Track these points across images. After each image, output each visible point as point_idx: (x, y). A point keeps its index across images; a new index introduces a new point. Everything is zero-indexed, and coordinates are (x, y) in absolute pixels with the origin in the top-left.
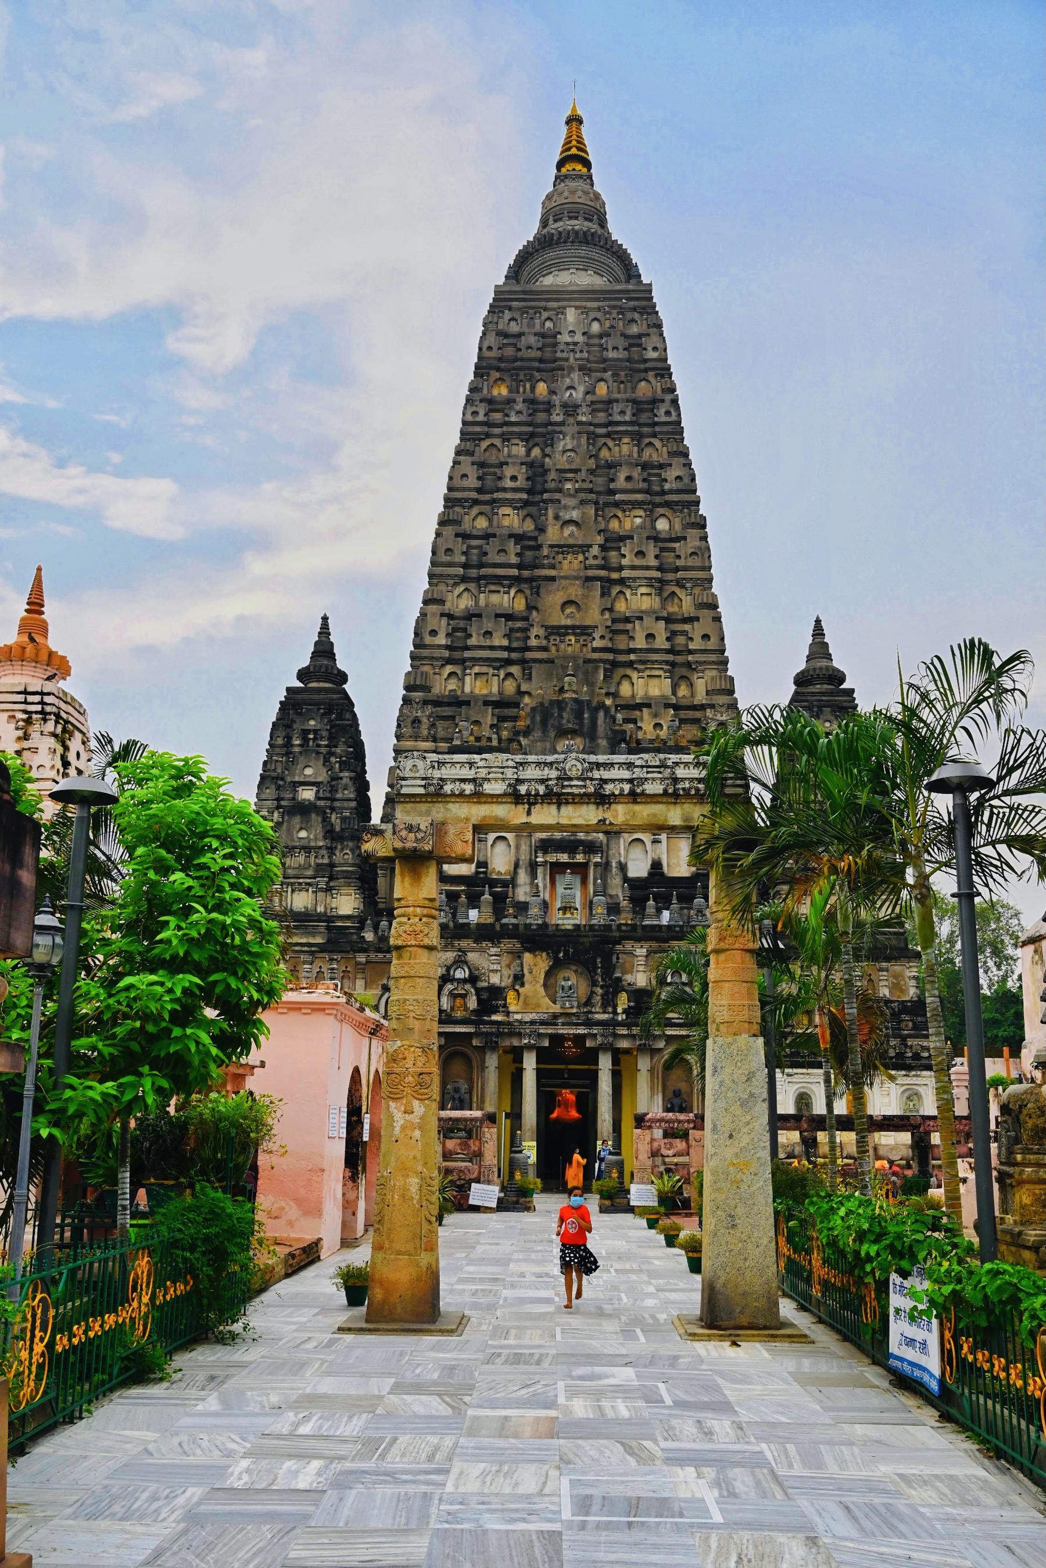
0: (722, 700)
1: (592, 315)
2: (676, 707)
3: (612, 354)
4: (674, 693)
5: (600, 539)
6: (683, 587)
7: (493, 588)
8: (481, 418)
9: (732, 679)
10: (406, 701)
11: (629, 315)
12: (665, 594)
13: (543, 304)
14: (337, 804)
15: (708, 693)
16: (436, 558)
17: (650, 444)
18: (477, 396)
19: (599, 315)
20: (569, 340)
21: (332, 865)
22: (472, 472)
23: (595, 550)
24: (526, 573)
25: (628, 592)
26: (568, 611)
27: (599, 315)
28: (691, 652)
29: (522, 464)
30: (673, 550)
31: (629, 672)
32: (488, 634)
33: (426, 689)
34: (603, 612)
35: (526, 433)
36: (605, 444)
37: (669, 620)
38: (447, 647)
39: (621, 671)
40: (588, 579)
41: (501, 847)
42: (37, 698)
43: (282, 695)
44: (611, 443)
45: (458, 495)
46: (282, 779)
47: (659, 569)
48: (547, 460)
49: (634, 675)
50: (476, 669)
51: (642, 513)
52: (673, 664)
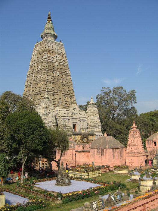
23: (61, 80)
40: (61, 84)
50: (50, 94)
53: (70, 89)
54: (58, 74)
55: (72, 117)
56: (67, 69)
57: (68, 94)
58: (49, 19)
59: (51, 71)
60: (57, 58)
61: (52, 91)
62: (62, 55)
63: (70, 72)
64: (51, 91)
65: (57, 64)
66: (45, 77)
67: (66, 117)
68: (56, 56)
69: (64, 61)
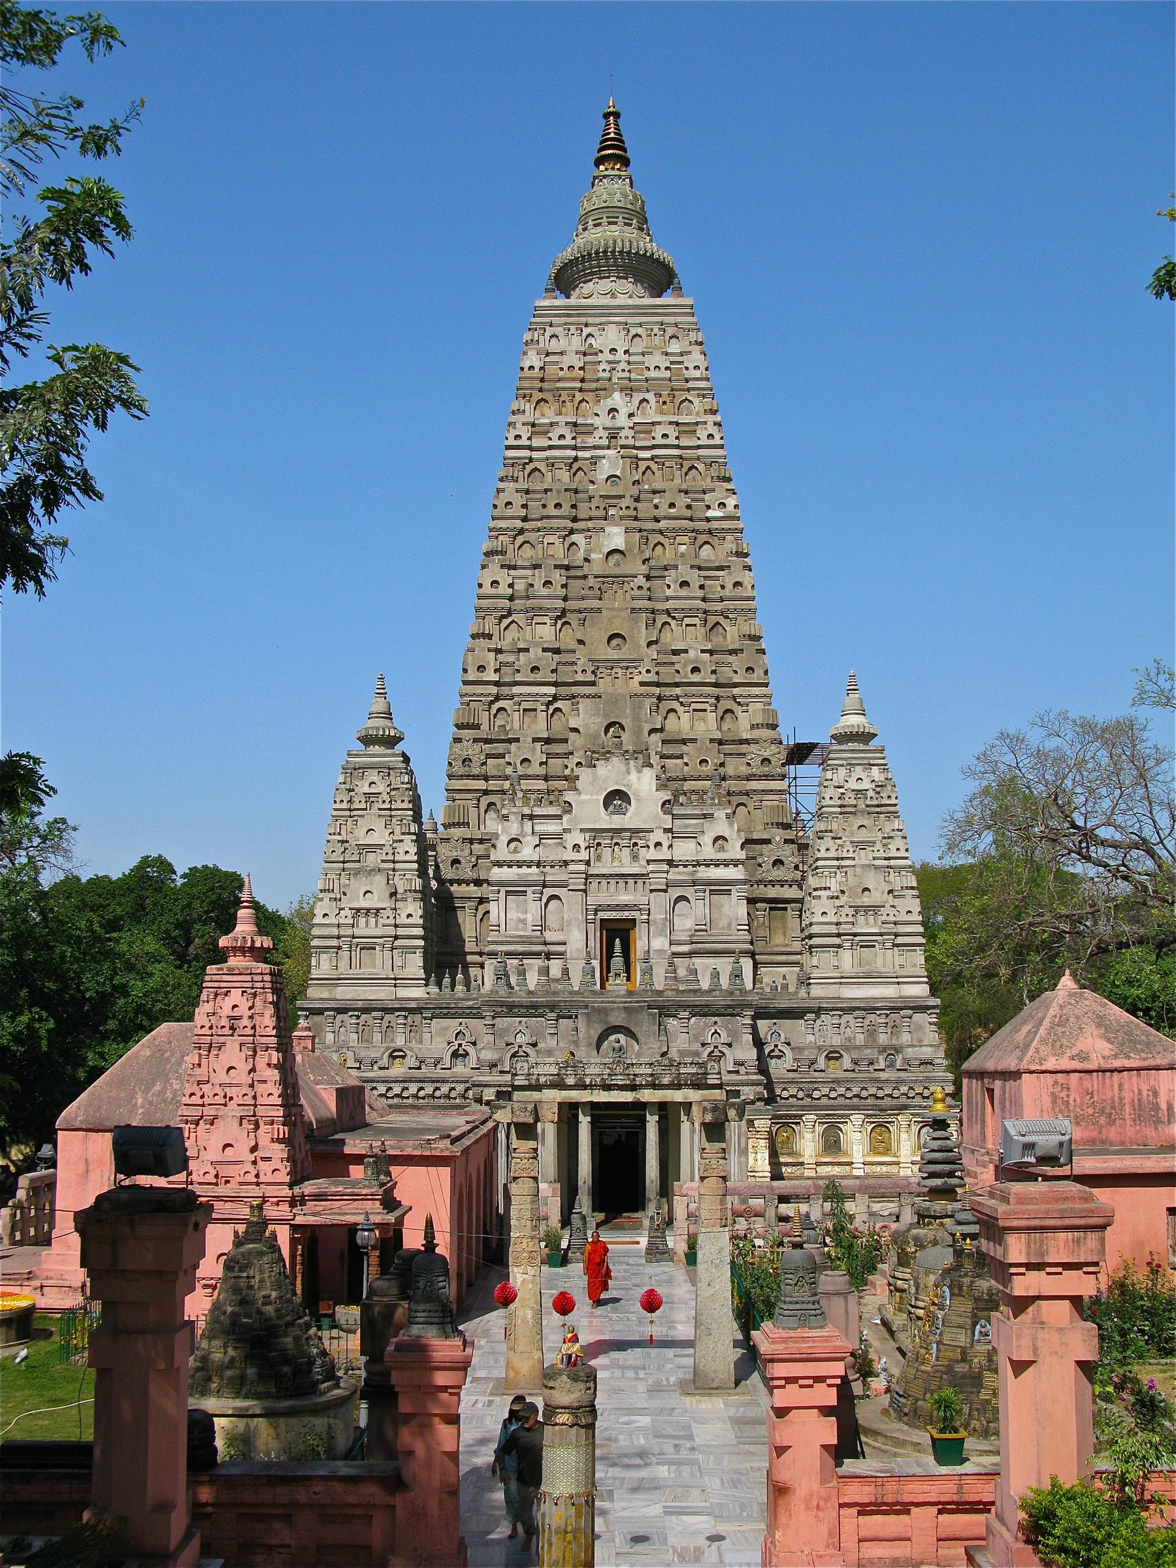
0: (766, 733)
1: (633, 331)
2: (720, 742)
3: (653, 374)
4: (719, 729)
5: (644, 569)
6: (727, 617)
7: (539, 619)
8: (524, 442)
9: (775, 714)
10: (457, 740)
11: (670, 331)
12: (709, 625)
13: (583, 320)
14: (398, 866)
15: (753, 727)
16: (481, 591)
17: (692, 467)
18: (520, 419)
19: (640, 331)
20: (611, 357)
21: (396, 926)
22: (518, 500)
23: (641, 580)
24: (572, 605)
25: (673, 623)
26: (614, 642)
27: (640, 331)
28: (736, 685)
29: (566, 490)
30: (717, 578)
31: (675, 705)
32: (535, 669)
33: (477, 727)
34: (649, 644)
35: (569, 458)
36: (648, 468)
37: (711, 652)
38: (497, 684)
39: (666, 705)
41: (553, 904)
42: (259, 978)
43: (343, 759)
44: (654, 467)
45: (503, 524)
46: (347, 842)
47: (704, 600)
48: (591, 487)
49: (680, 709)
50: (525, 705)
51: (686, 539)
52: (718, 698)
53: (732, 635)
54: (615, 537)
55: (588, 863)
56: (707, 483)
57: (696, 678)
58: (614, 153)
59: (551, 531)
60: (622, 420)
61: (538, 677)
62: (674, 391)
63: (731, 502)
64: (532, 677)
65: (610, 463)
66: (487, 584)
67: (525, 870)
68: (613, 410)
69: (689, 429)
